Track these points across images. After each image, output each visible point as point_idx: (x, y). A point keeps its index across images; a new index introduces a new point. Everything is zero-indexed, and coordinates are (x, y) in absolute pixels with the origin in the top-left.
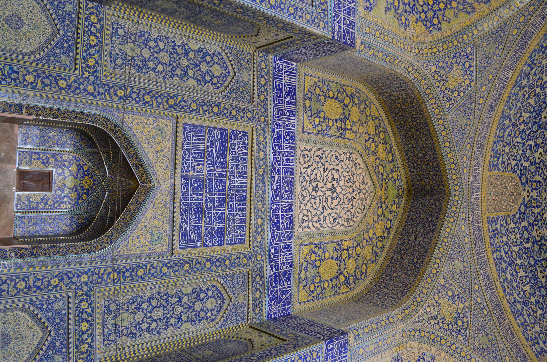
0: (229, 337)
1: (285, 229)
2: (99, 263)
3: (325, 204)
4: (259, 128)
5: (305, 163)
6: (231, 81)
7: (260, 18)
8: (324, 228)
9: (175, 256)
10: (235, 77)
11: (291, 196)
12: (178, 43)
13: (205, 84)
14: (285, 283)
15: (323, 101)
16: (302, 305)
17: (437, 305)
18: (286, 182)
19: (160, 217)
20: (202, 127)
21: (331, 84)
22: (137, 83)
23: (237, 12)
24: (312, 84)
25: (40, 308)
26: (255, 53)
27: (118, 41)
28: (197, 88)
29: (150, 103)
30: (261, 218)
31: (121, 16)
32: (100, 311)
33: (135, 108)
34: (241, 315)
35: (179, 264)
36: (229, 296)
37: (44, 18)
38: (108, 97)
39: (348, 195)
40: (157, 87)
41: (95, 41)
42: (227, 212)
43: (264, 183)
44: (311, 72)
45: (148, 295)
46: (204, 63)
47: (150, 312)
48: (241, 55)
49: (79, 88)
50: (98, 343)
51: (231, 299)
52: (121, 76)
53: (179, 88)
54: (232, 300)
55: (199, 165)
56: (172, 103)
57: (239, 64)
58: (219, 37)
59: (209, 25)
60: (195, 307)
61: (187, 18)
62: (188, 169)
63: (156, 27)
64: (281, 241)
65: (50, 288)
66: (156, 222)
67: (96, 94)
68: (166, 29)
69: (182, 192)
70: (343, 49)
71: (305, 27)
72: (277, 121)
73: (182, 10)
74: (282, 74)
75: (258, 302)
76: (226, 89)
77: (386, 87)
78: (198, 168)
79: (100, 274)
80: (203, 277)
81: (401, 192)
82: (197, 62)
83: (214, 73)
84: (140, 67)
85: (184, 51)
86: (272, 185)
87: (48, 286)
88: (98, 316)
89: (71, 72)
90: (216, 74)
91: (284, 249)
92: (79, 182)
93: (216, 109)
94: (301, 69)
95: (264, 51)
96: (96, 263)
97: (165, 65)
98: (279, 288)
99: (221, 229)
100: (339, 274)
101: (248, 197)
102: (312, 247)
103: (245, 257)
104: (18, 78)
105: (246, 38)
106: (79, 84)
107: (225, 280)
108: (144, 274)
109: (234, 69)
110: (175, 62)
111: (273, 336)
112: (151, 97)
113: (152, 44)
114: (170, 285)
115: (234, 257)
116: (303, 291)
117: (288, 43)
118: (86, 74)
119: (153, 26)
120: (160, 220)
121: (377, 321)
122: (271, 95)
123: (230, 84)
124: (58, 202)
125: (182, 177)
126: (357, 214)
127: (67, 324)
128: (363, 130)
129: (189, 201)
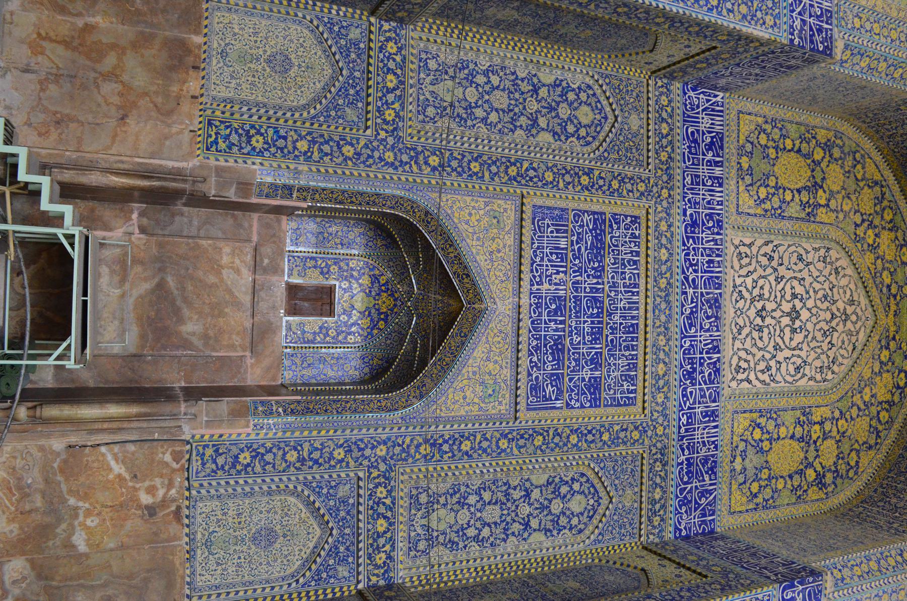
0: (608, 562)
1: (706, 384)
2: (403, 429)
3: (779, 340)
4: (660, 209)
5: (741, 267)
6: (610, 131)
7: (657, 20)
8: (778, 382)
9: (521, 422)
10: (616, 125)
11: (717, 326)
12: (521, 75)
13: (566, 140)
15: (773, 156)
16: (736, 516)
18: (708, 301)
19: (496, 358)
20: (563, 210)
21: (789, 126)
22: (459, 144)
23: (619, 14)
24: (753, 127)
25: (319, 493)
26: (650, 82)
27: (428, 79)
28: (553, 147)
29: (480, 175)
30: (664, 363)
31: (432, 40)
32: (404, 503)
33: (456, 184)
34: (627, 526)
35: (526, 436)
36: (608, 493)
37: (320, 53)
38: (415, 168)
39: (823, 325)
40: (490, 148)
41: (395, 81)
42: (605, 352)
43: (668, 302)
44: (749, 106)
45: (477, 483)
46: (565, 105)
47: (480, 511)
48: (627, 86)
49: (372, 157)
50: (400, 553)
51: (611, 498)
52: (434, 134)
53: (525, 147)
54: (614, 500)
55: (558, 273)
56: (514, 173)
57: (622, 102)
58: (588, 60)
59: (571, 40)
60: (552, 507)
61: (536, 33)
62: (541, 280)
63: (486, 52)
64: (699, 403)
65: (333, 463)
66: (491, 366)
67: (397, 164)
68: (502, 54)
69: (531, 317)
70: (812, 61)
71: (738, 27)
72: (691, 196)
73: (527, 20)
74: (698, 113)
75: (657, 506)
76: (601, 145)
77: (894, 125)
78: (556, 278)
79: (405, 446)
80: (565, 458)
82: (553, 104)
83: (581, 120)
84: (462, 119)
85: (531, 88)
86: (683, 306)
87: (330, 459)
88: (401, 510)
89: (361, 132)
90: (585, 121)
92: (374, 302)
93: (585, 180)
94: (732, 103)
95: (665, 77)
96: (399, 428)
97: (501, 113)
98: (694, 485)
99: (595, 381)
100: (806, 467)
101: (642, 326)
102: (755, 415)
103: (636, 428)
104: (286, 146)
105: (634, 56)
106: (373, 151)
107: (602, 465)
108: (472, 448)
109: (614, 111)
110: (517, 106)
111: (684, 566)
112: (481, 165)
113: (480, 79)
114: (512, 469)
115: (616, 428)
116: (739, 493)
117: (707, 59)
118: (383, 134)
119: (482, 50)
120: (496, 362)
121: (879, 556)
122: (678, 151)
123: (608, 135)
124: (343, 332)
125: (531, 293)
126: (840, 359)
127: (355, 519)
128: (850, 206)
129: (543, 333)
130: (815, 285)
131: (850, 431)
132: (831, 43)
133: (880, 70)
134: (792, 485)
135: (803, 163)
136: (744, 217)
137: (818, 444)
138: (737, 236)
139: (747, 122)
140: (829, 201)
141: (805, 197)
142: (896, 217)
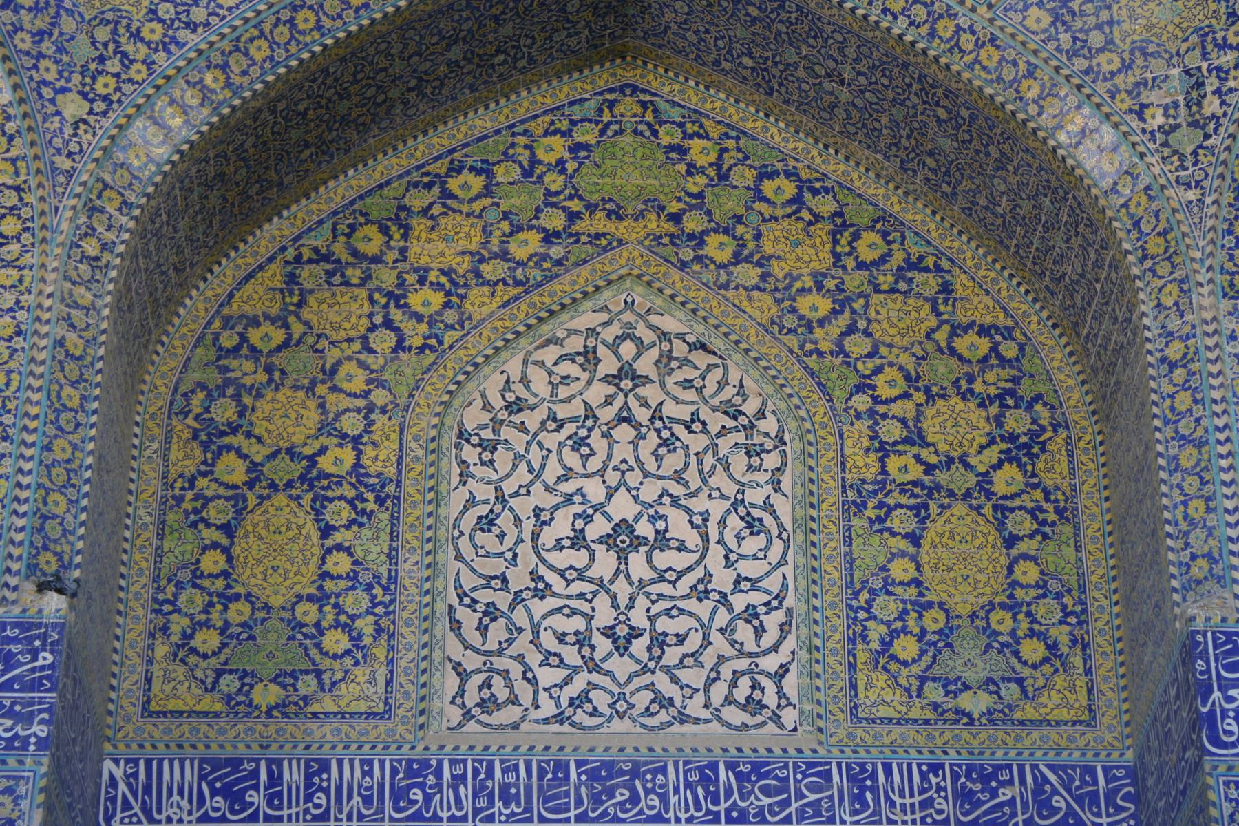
1: (786, 804)
5: (514, 700)
8: (784, 586)
11: (654, 772)
14: (1005, 794)
15: (246, 608)
16: (1100, 703)
17: (1139, 62)
18: (596, 800)
24: (180, 671)
44: (131, 681)
81: (628, 106)
91: (865, 805)
100: (989, 495)
102: (862, 657)
121: (1169, 432)
130: (550, 476)
131: (906, 360)
132: (32, 626)
133: (67, 455)
134: (1031, 536)
135: (257, 517)
136: (398, 696)
137: (933, 460)
138: (441, 713)
139: (168, 688)
140: (344, 436)
141: (339, 513)
142: (374, 215)
